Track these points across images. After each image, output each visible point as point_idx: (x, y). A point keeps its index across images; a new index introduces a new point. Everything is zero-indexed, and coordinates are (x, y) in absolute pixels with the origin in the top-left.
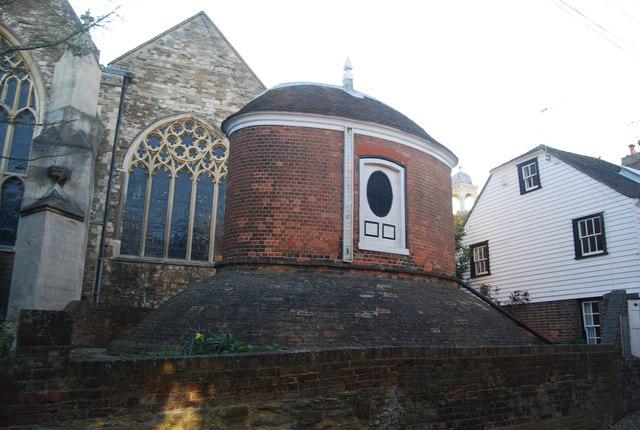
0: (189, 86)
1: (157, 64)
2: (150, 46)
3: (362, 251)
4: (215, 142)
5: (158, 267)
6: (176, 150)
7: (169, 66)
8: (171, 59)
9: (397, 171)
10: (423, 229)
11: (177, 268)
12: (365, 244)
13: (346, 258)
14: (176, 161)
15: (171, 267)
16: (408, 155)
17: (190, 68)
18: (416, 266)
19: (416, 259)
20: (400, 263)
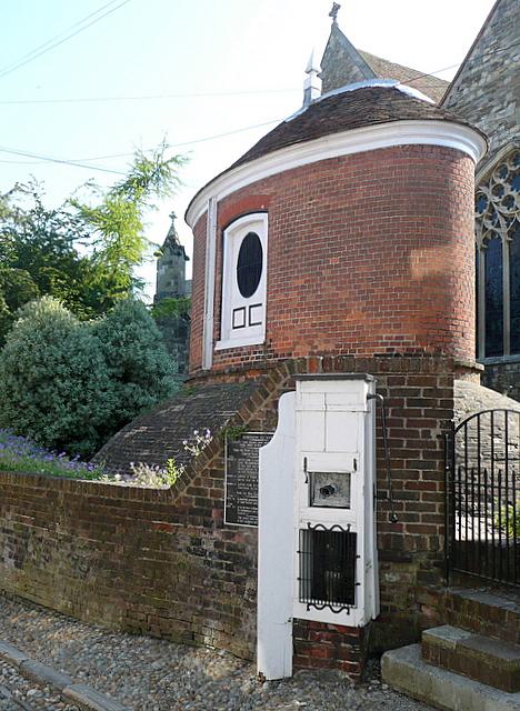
0: (505, 104)
1: (468, 100)
2: (459, 80)
3: (219, 351)
4: (492, 187)
5: (495, 369)
6: (504, 203)
7: (480, 93)
8: (482, 82)
9: (262, 221)
10: (293, 294)
11: (515, 366)
12: (233, 339)
13: (208, 365)
14: (506, 219)
15: (508, 367)
16: (272, 190)
17: (504, 78)
18: (276, 356)
19: (278, 347)
20: (253, 358)
